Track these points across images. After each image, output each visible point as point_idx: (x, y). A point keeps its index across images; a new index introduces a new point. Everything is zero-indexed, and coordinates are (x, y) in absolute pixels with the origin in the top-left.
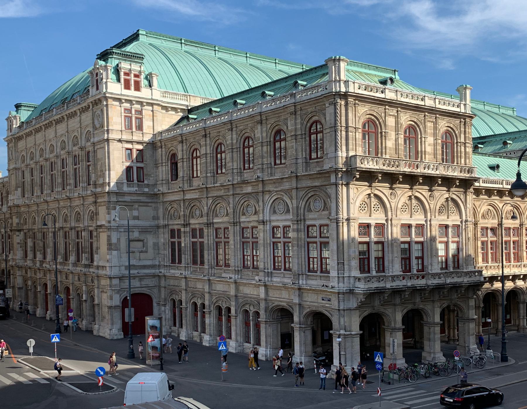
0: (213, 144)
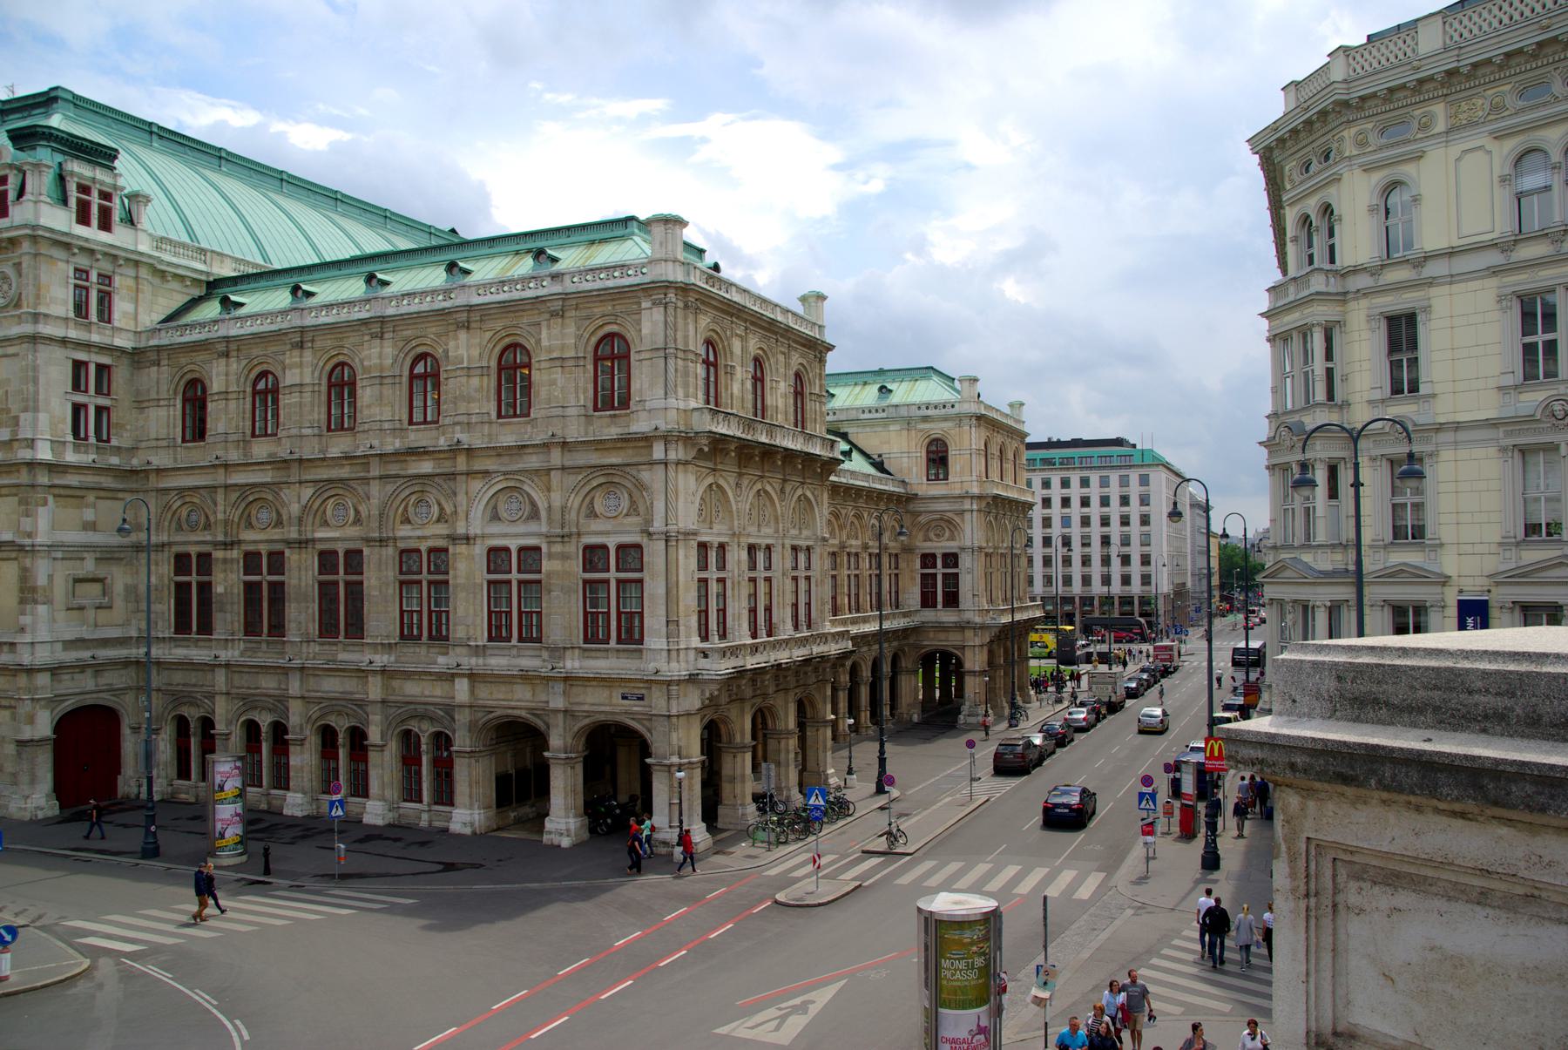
0: (321, 364)
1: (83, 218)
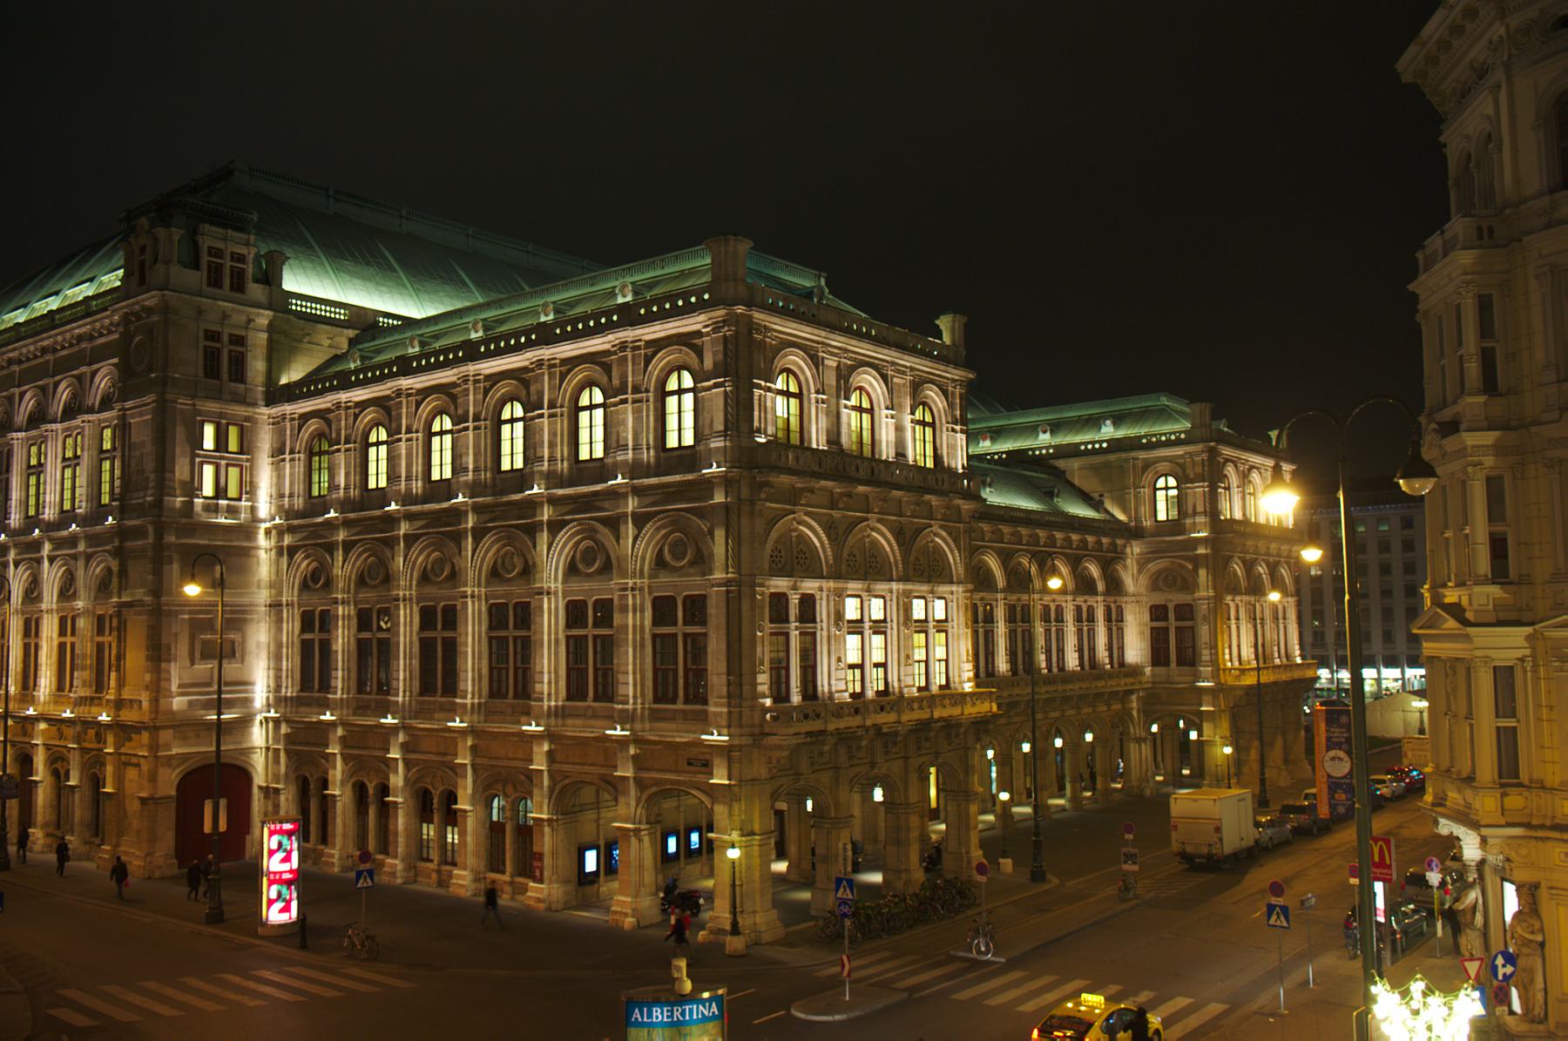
1: (215, 280)
